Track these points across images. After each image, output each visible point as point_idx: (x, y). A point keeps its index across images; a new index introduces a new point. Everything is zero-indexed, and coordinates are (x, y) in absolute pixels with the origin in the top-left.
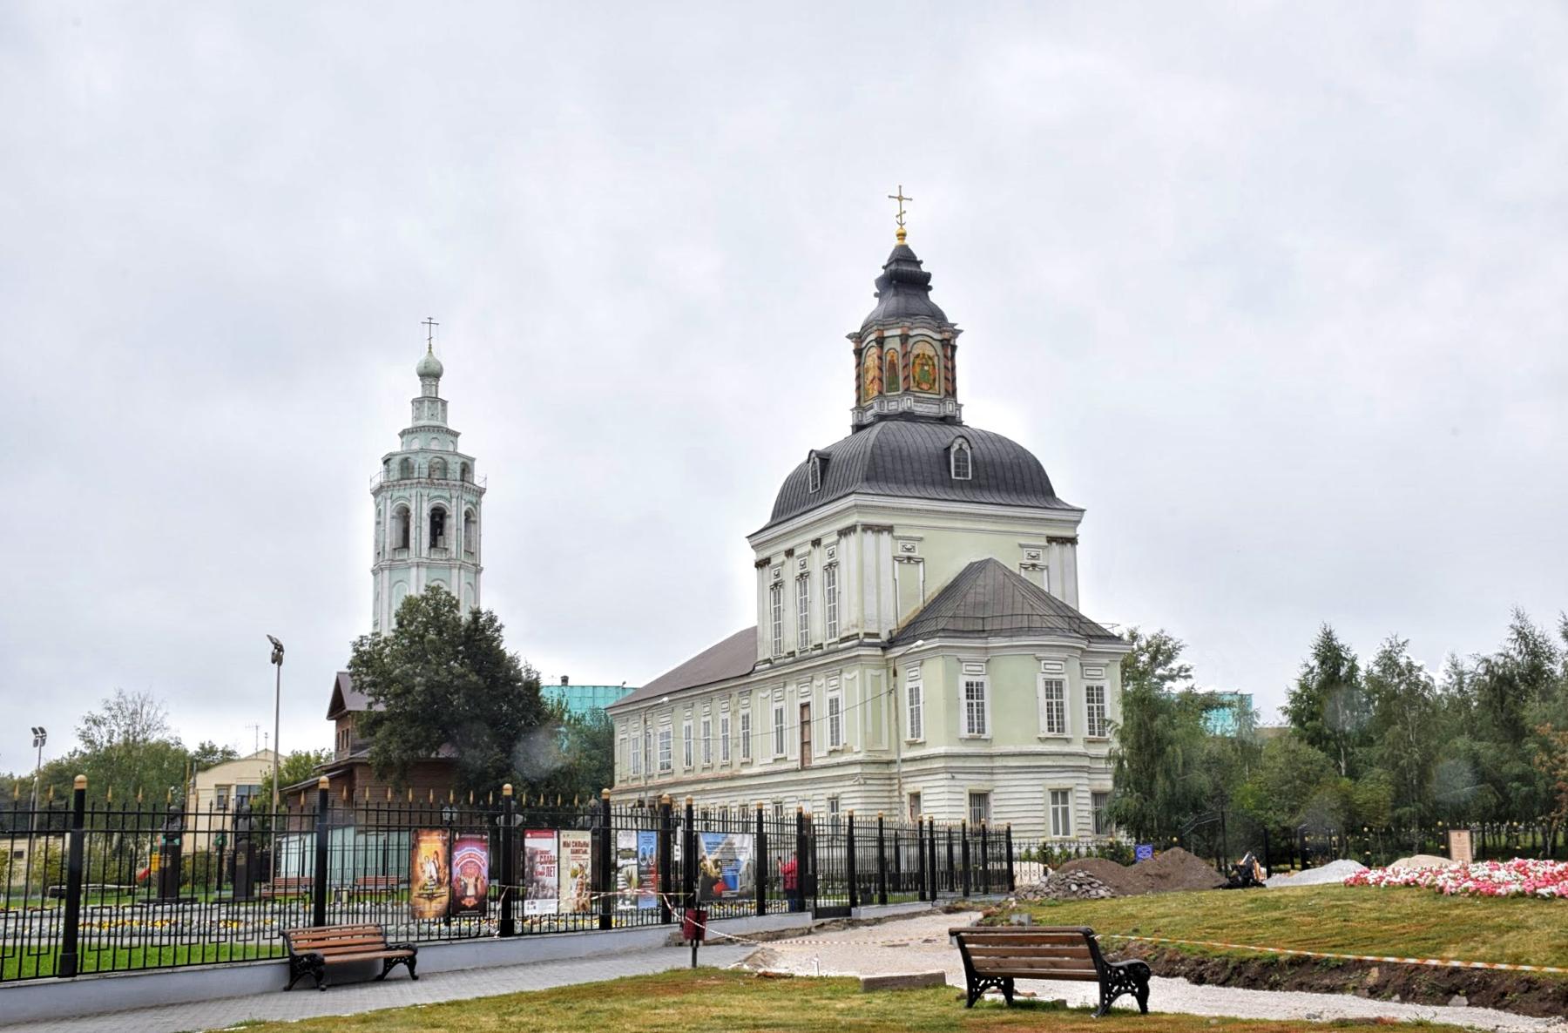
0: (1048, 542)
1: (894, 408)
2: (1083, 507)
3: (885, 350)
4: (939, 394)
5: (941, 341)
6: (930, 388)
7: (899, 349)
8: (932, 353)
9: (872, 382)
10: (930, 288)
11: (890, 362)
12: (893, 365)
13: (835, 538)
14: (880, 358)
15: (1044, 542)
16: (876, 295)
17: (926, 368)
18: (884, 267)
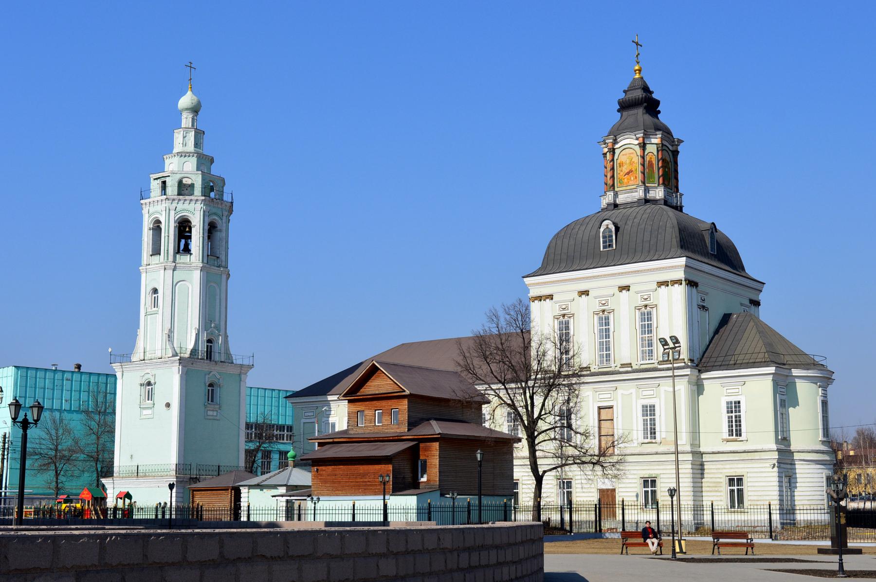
0: (751, 303)
1: (652, 195)
2: (765, 282)
3: (646, 153)
4: (672, 190)
5: (673, 152)
6: (668, 185)
7: (656, 154)
8: (668, 159)
9: (628, 173)
10: (659, 112)
11: (649, 161)
12: (650, 163)
13: (655, 286)
14: (643, 157)
15: (747, 302)
16: (619, 111)
17: (667, 170)
18: (625, 92)
